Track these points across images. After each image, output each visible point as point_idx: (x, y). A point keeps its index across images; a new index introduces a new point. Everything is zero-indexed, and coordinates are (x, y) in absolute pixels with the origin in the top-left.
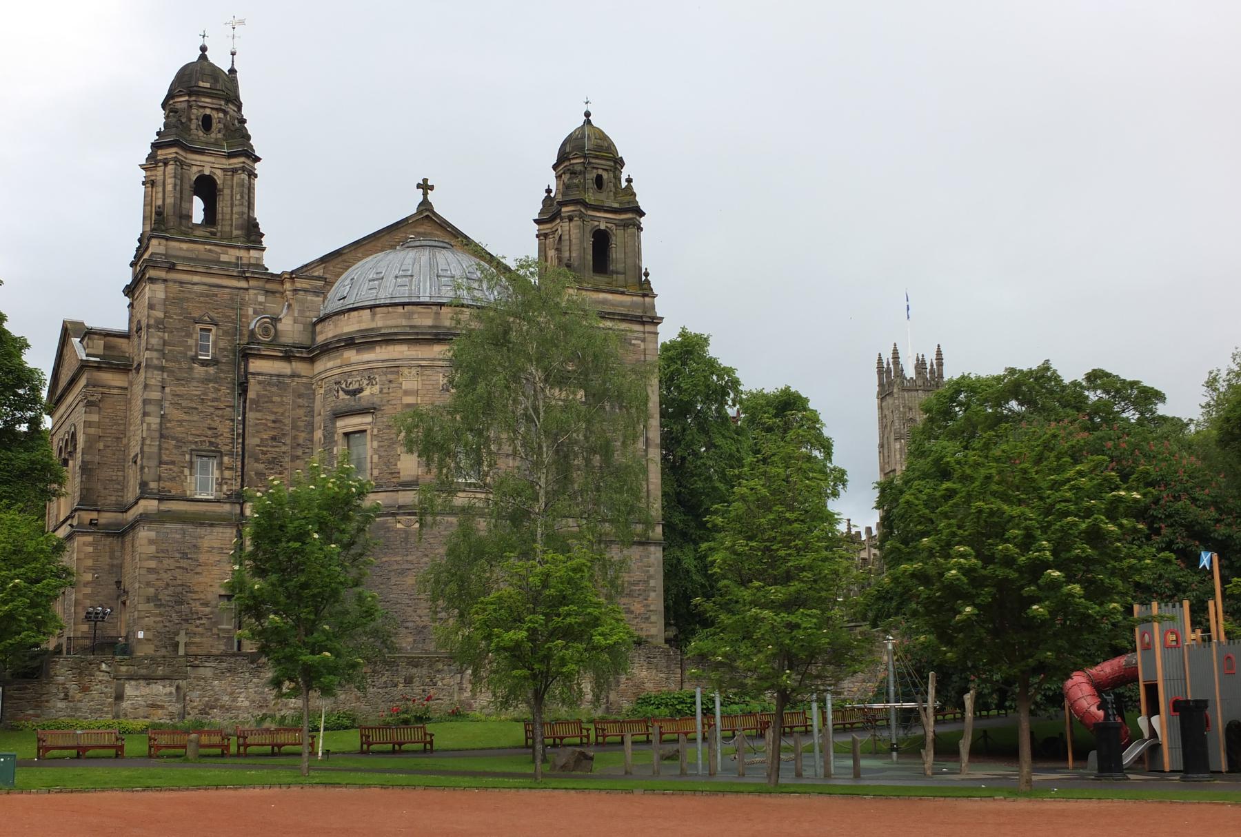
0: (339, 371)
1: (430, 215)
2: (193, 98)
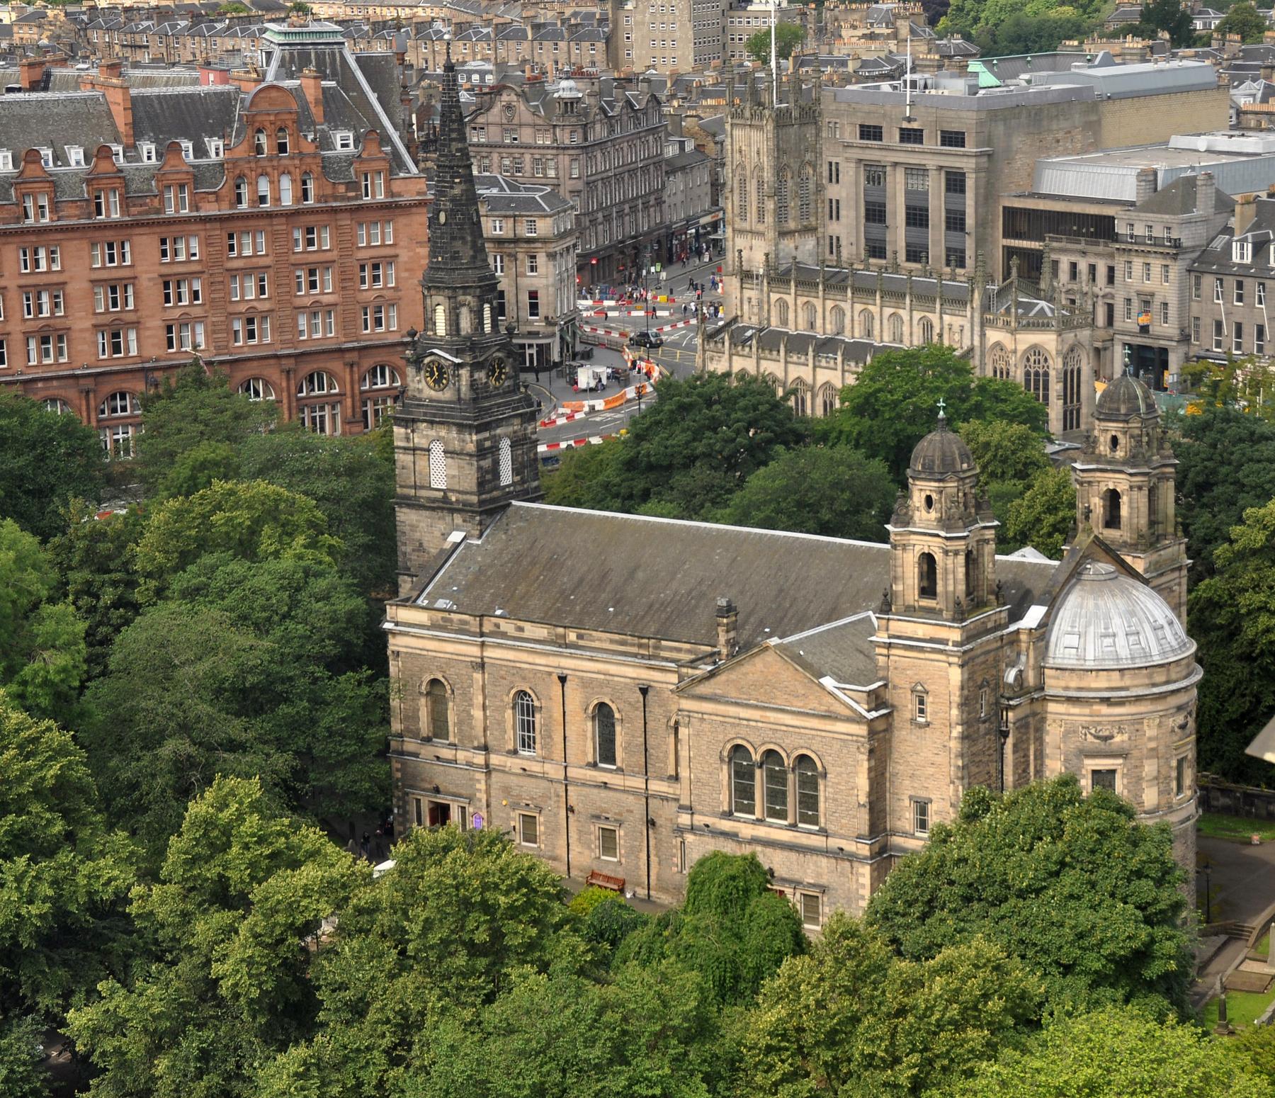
0: (1088, 719)
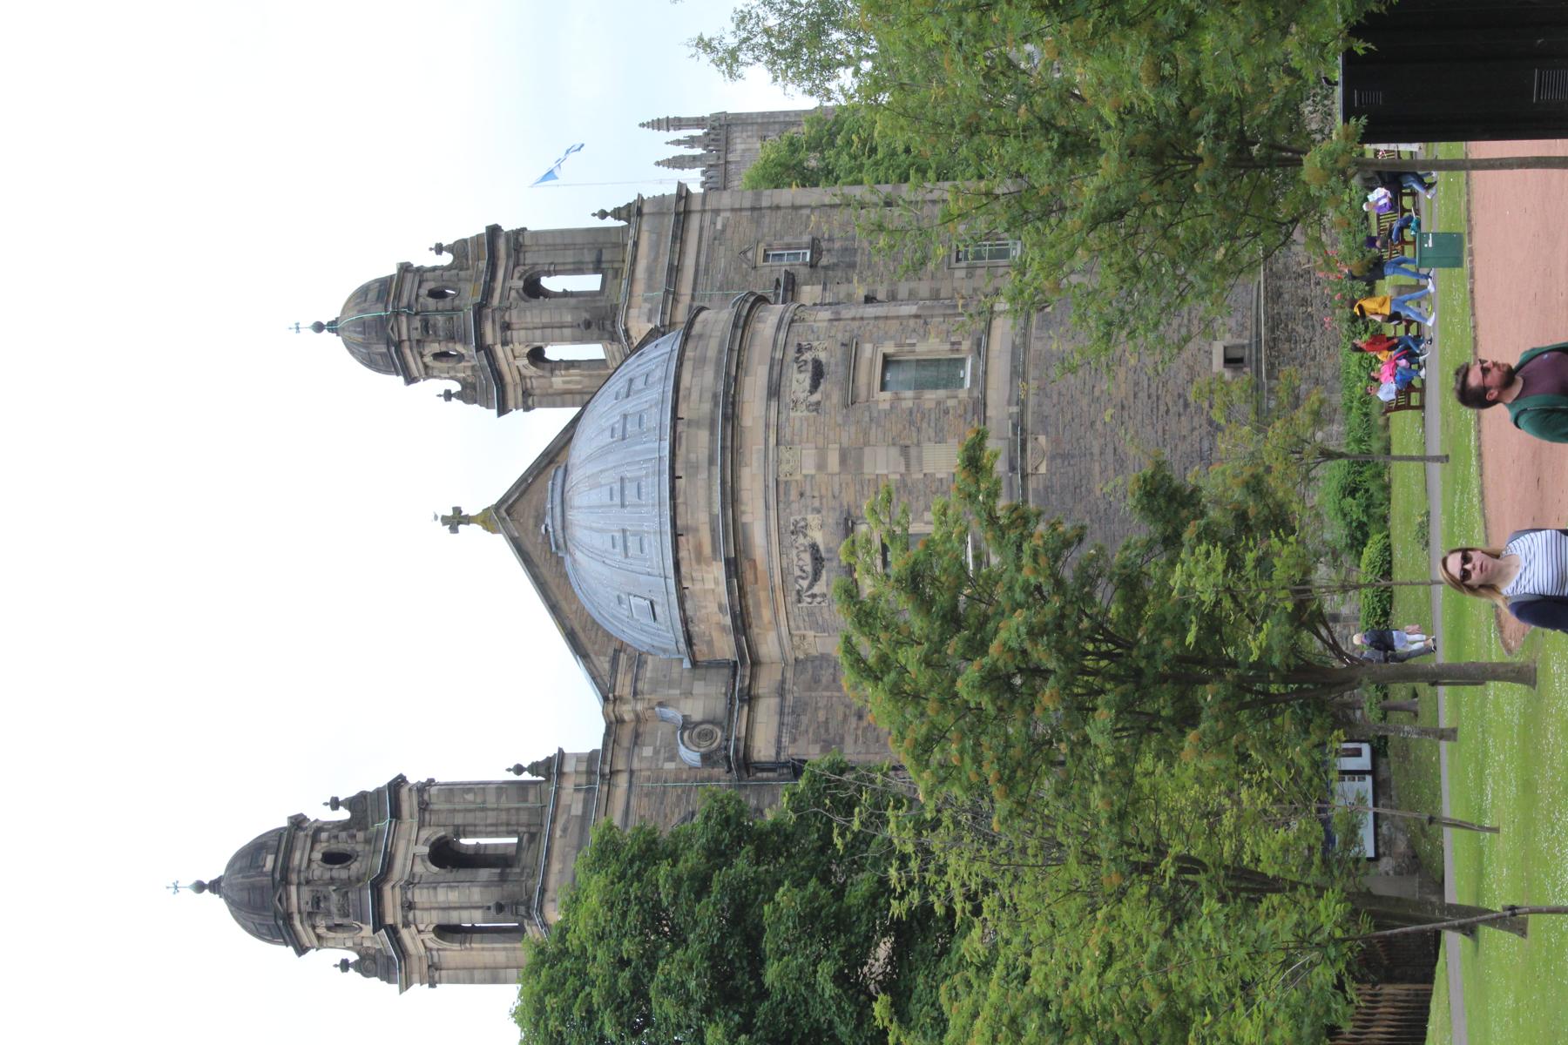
1: (505, 506)
2: (294, 877)
